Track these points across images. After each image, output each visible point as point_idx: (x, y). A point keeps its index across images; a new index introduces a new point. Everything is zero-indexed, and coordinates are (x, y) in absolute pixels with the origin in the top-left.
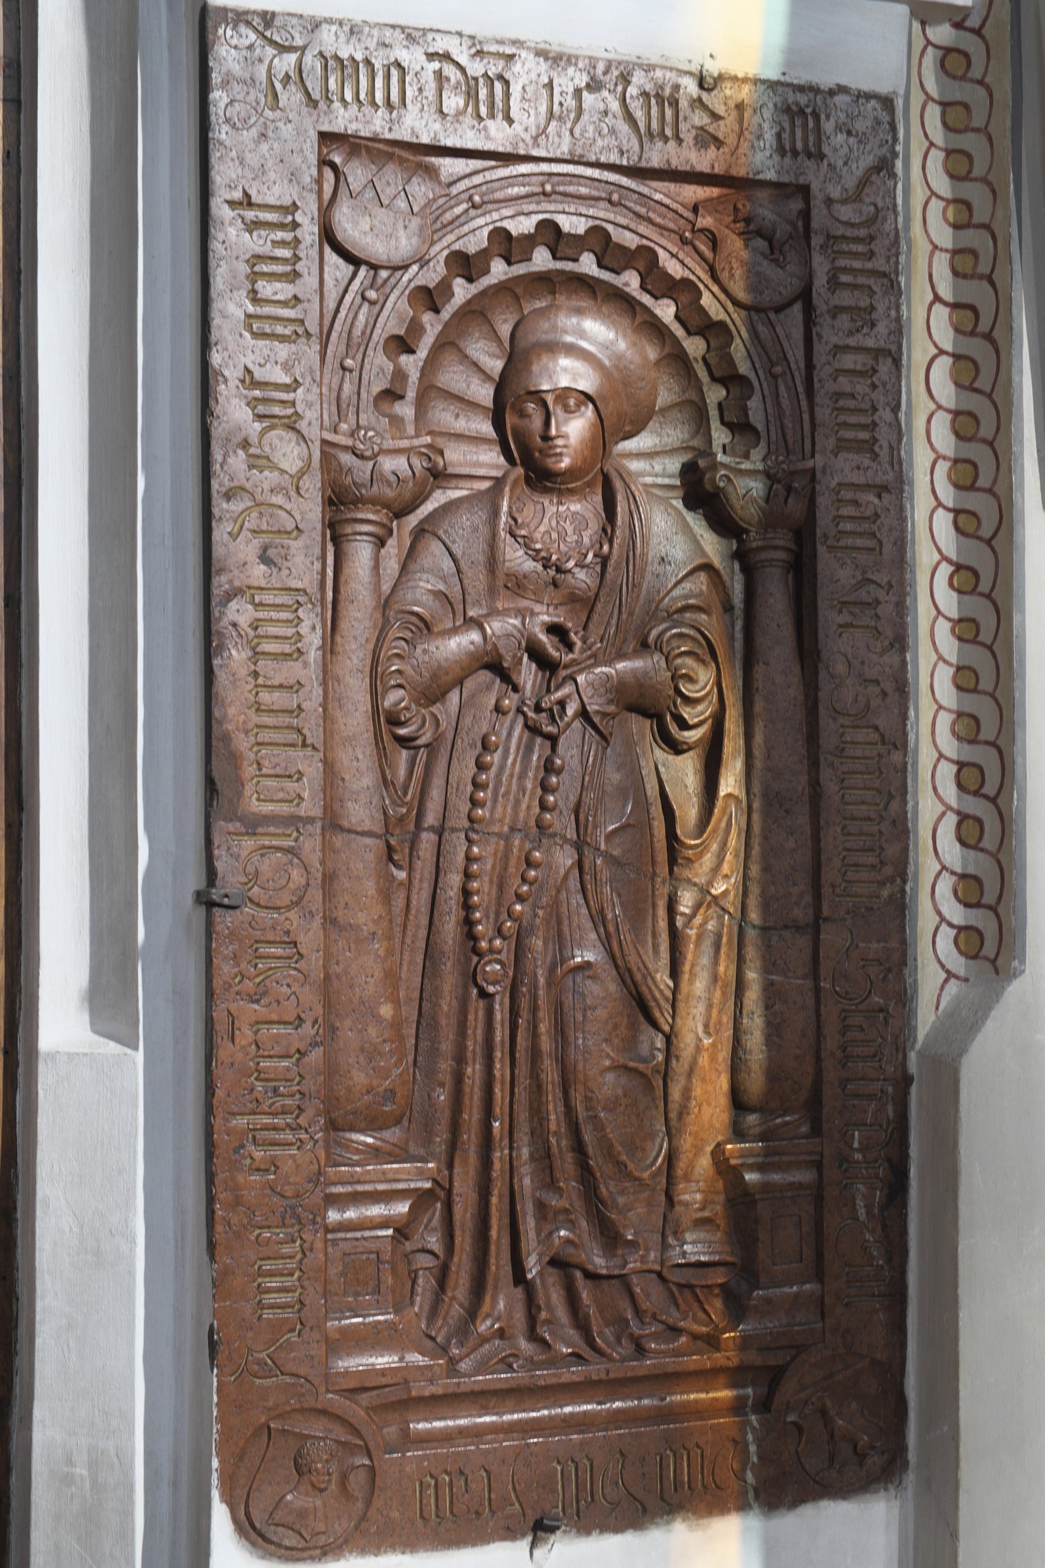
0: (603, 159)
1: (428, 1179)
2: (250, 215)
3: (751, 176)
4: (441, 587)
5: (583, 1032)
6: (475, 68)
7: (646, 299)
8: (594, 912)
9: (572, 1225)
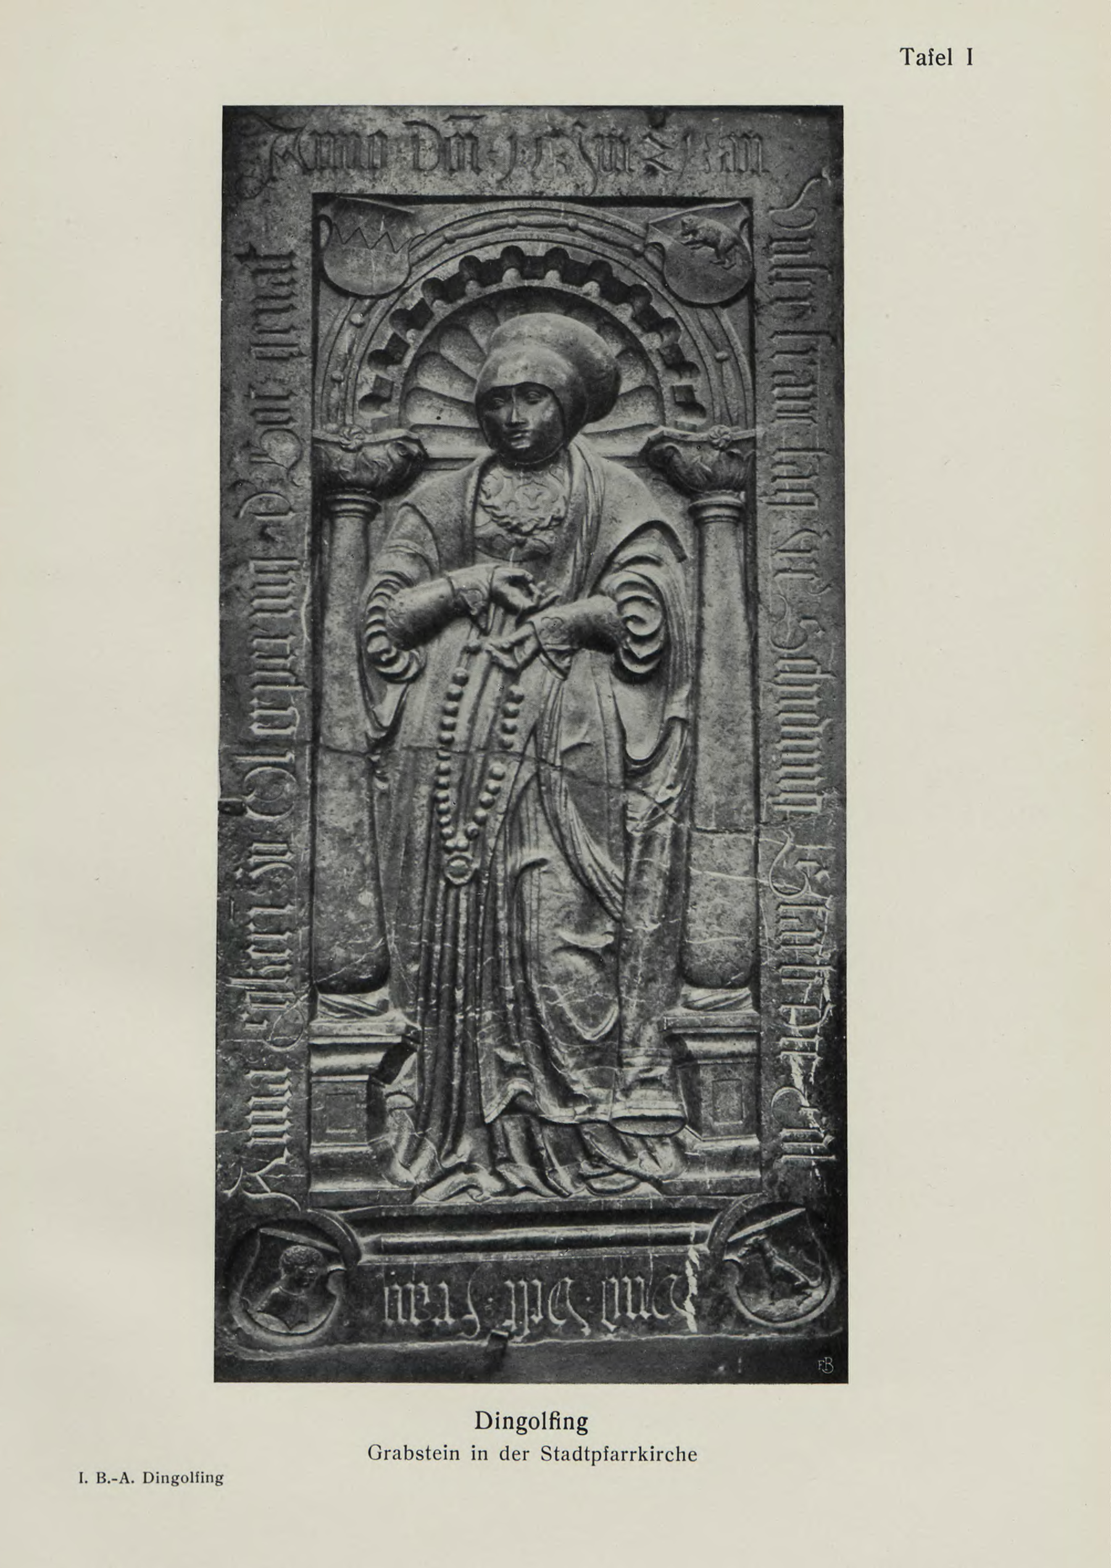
0: (561, 193)
1: (398, 1035)
2: (253, 265)
3: (697, 195)
4: (418, 549)
5: (538, 918)
6: (449, 130)
7: (605, 304)
8: (549, 817)
9: (529, 1077)
